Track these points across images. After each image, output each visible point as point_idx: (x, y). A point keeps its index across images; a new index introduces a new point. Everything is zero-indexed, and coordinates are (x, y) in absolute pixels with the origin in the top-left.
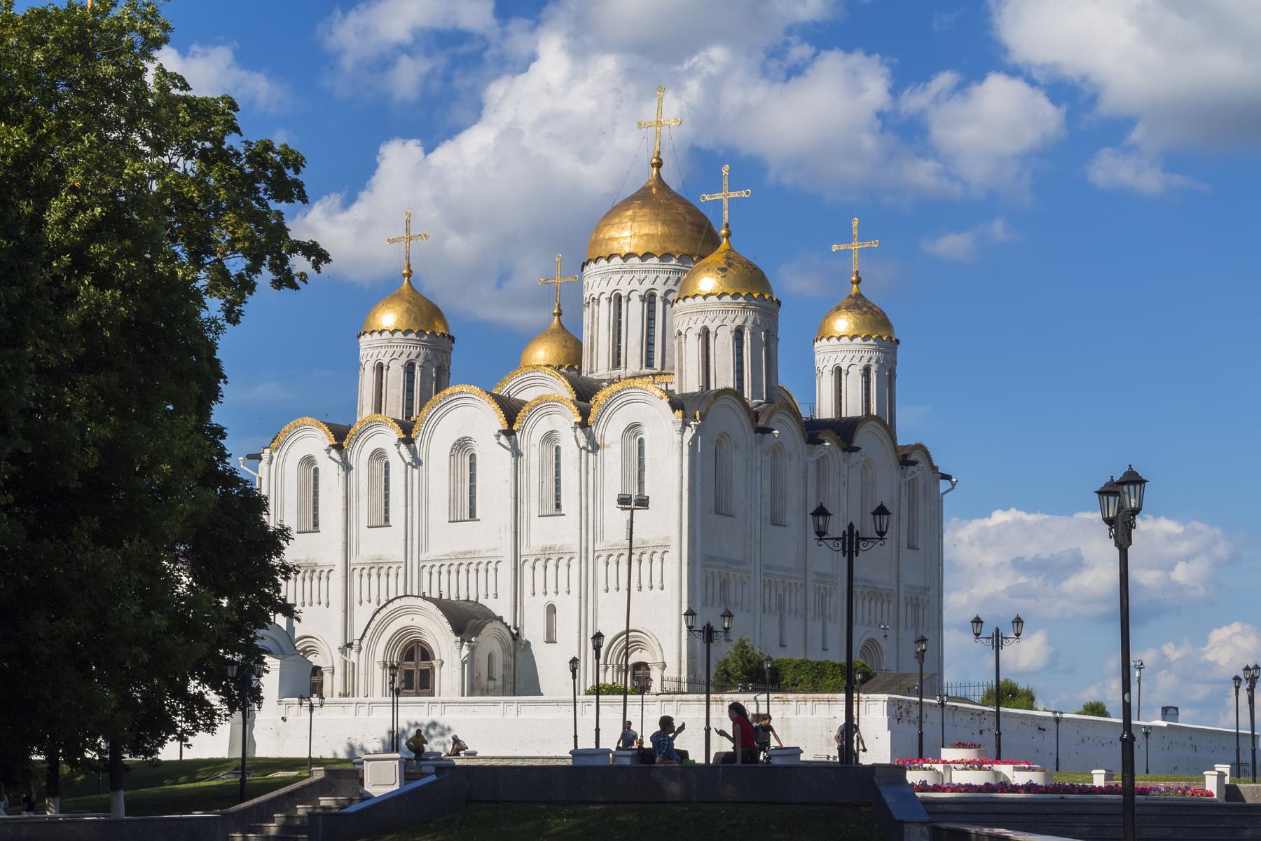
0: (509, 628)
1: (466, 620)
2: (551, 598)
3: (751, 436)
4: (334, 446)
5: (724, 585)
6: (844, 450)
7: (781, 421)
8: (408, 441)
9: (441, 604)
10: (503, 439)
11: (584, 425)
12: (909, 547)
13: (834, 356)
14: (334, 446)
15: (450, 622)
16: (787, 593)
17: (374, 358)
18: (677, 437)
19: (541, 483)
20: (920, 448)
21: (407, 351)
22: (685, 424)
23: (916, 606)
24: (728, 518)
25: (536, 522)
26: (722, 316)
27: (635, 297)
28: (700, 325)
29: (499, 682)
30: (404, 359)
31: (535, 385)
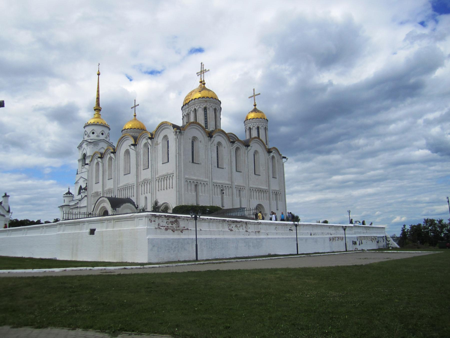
0: (134, 205)
3: (207, 139)
6: (246, 146)
7: (220, 135)
10: (132, 147)
14: (99, 157)
15: (111, 204)
18: (175, 137)
19: (144, 159)
20: (275, 148)
22: (176, 132)
23: (276, 194)
24: (197, 165)
25: (142, 171)
26: (199, 105)
28: (193, 108)
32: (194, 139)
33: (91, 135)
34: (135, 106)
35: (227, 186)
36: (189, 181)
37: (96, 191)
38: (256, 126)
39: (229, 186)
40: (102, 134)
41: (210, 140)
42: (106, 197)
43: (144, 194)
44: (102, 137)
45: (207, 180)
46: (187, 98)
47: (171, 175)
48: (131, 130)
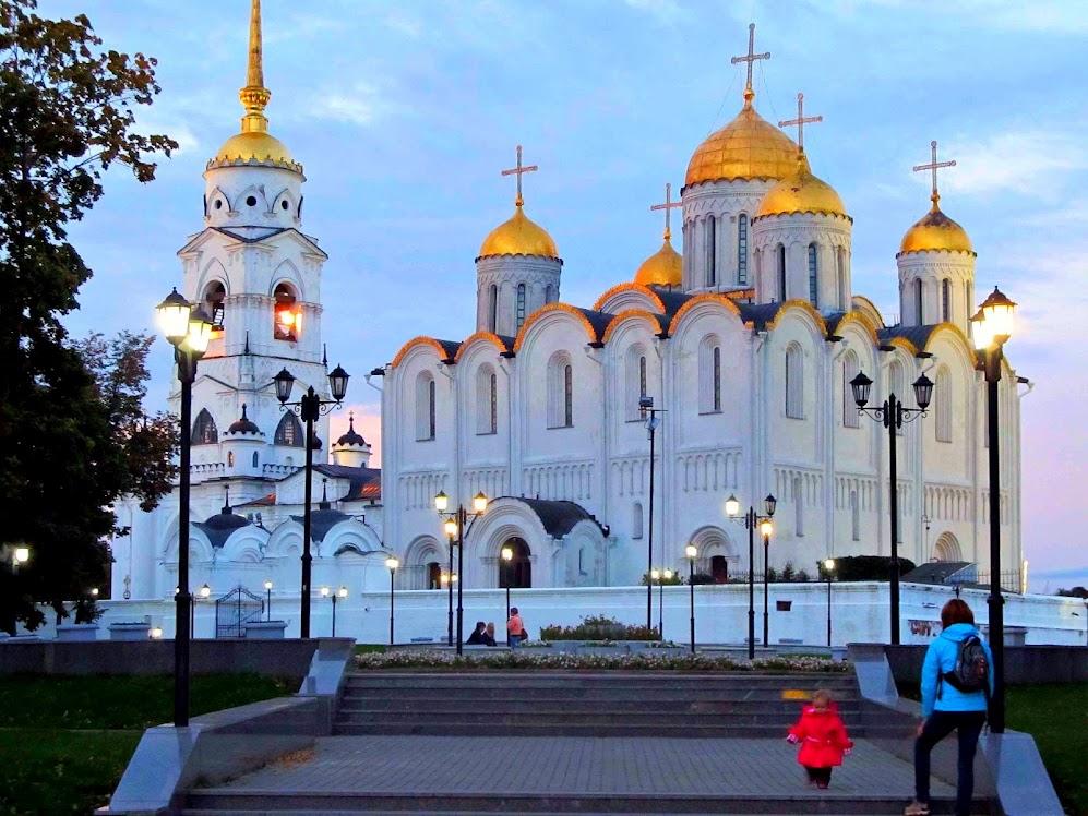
0: (600, 526)
1: (559, 518)
2: (637, 498)
4: (445, 362)
5: (797, 482)
7: (852, 330)
8: (510, 354)
9: (530, 502)
10: (592, 349)
11: (664, 336)
12: (937, 440)
13: (914, 269)
14: (445, 362)
15: (543, 520)
16: (861, 490)
17: (488, 281)
18: (748, 347)
21: (518, 273)
27: (726, 218)
29: (591, 576)
30: (515, 282)
31: (630, 302)
32: (793, 348)
33: (245, 208)
34: (520, 171)
35: (866, 479)
36: (781, 469)
37: (421, 466)
38: (941, 278)
39: (873, 480)
40: (285, 205)
41: (828, 350)
42: (522, 499)
43: (632, 494)
44: (284, 218)
45: (818, 465)
46: (709, 158)
47: (733, 452)
48: (518, 259)
